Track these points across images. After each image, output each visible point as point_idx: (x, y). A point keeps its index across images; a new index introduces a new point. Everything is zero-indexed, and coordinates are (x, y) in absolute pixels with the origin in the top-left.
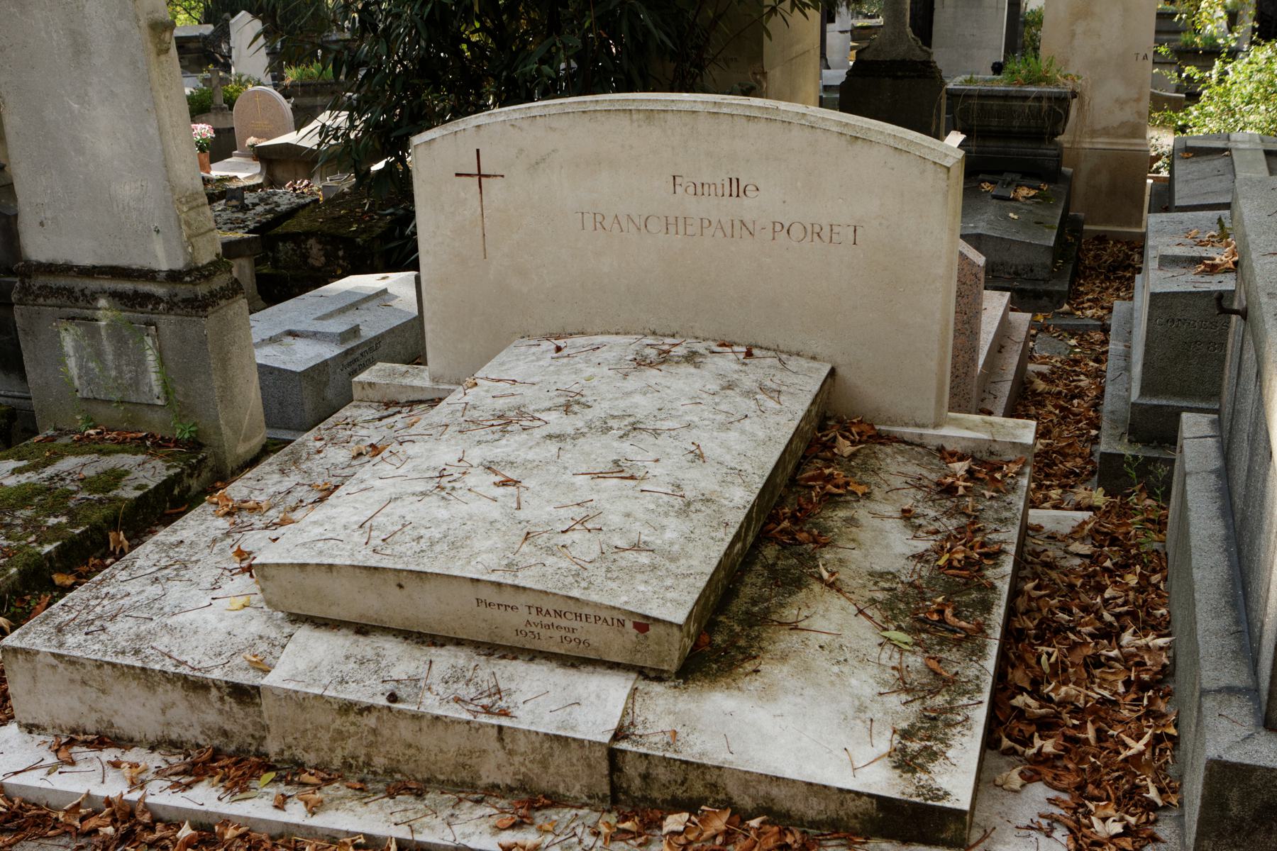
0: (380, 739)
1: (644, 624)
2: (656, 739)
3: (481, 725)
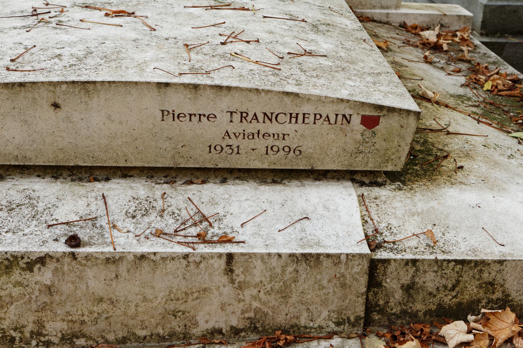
0: (57, 298)
1: (373, 117)
2: (413, 243)
3: (204, 257)
